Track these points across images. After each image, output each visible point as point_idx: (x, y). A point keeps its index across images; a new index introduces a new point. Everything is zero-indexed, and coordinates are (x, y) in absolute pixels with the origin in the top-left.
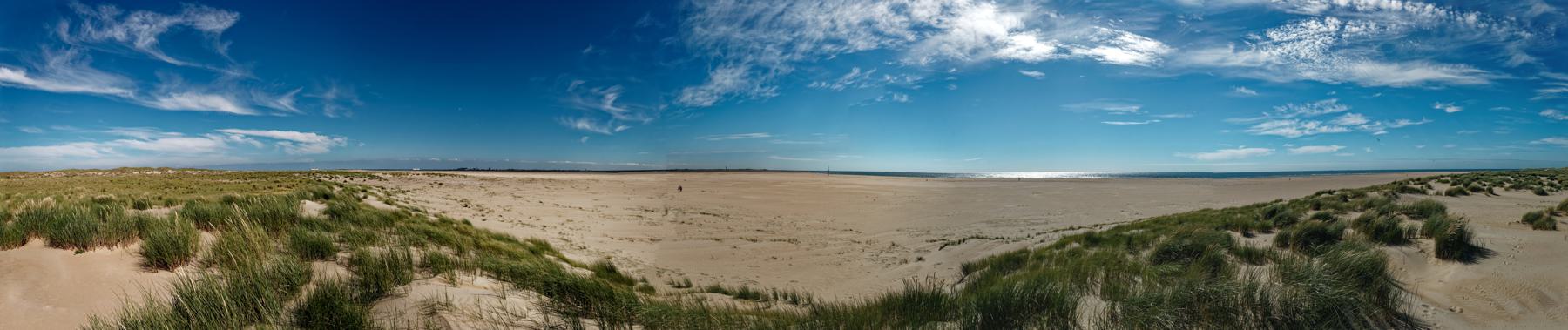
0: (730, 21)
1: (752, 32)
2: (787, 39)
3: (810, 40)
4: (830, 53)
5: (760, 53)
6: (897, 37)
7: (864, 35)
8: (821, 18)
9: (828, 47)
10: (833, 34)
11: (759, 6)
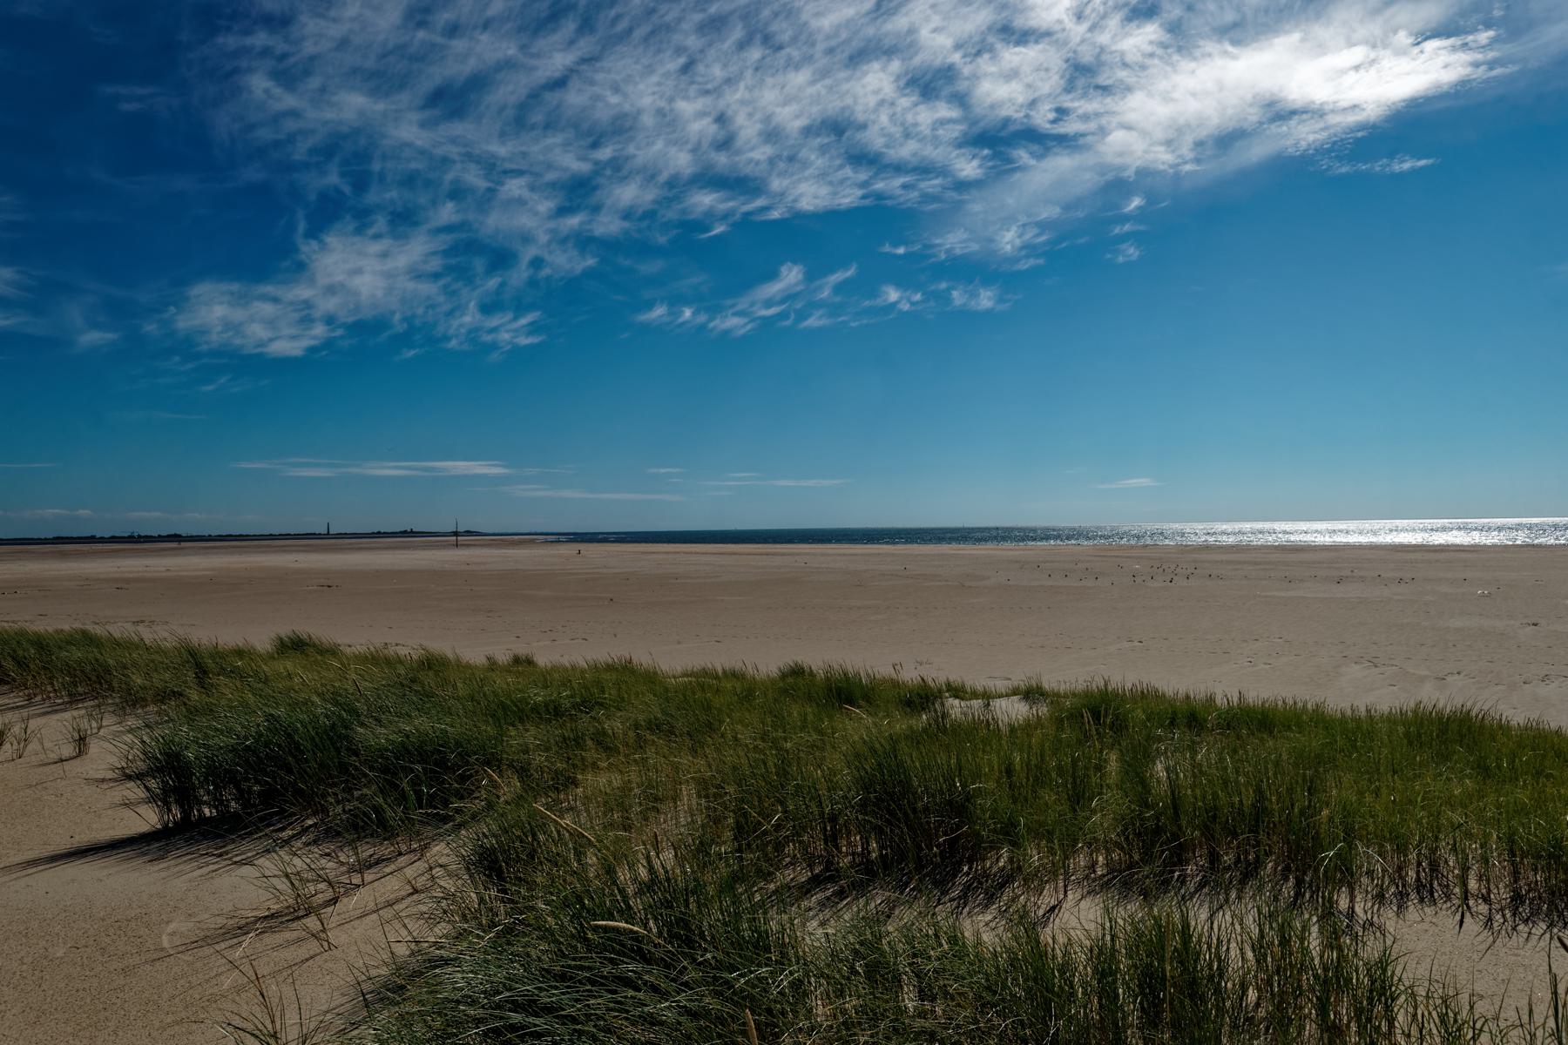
0: (382, 77)
1: (458, 128)
2: (573, 163)
3: (649, 175)
4: (710, 216)
5: (487, 199)
6: (925, 169)
7: (820, 162)
8: (685, 107)
9: (705, 200)
10: (721, 160)
11: (489, 48)
